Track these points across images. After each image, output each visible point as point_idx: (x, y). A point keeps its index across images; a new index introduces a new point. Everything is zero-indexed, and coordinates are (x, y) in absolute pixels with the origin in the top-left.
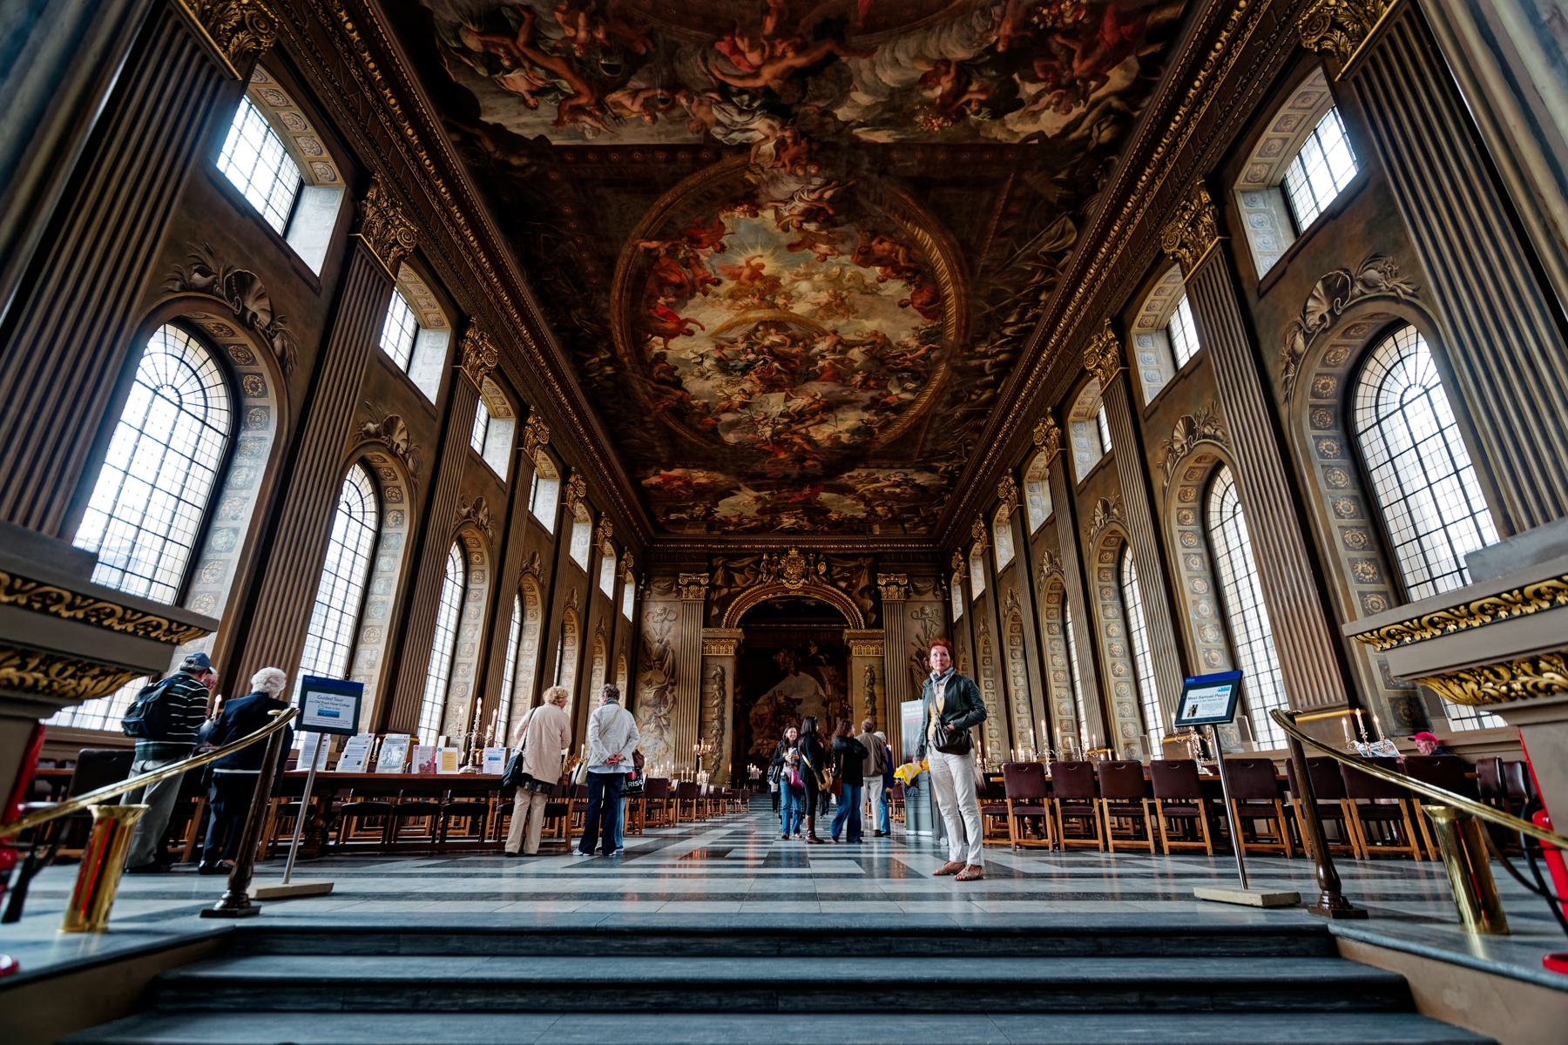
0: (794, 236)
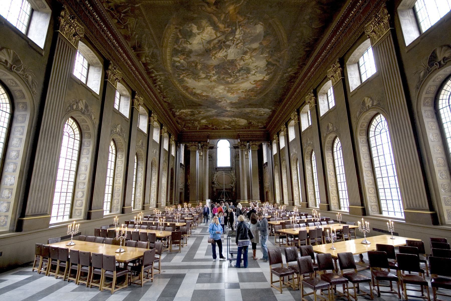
0: (223, 99)
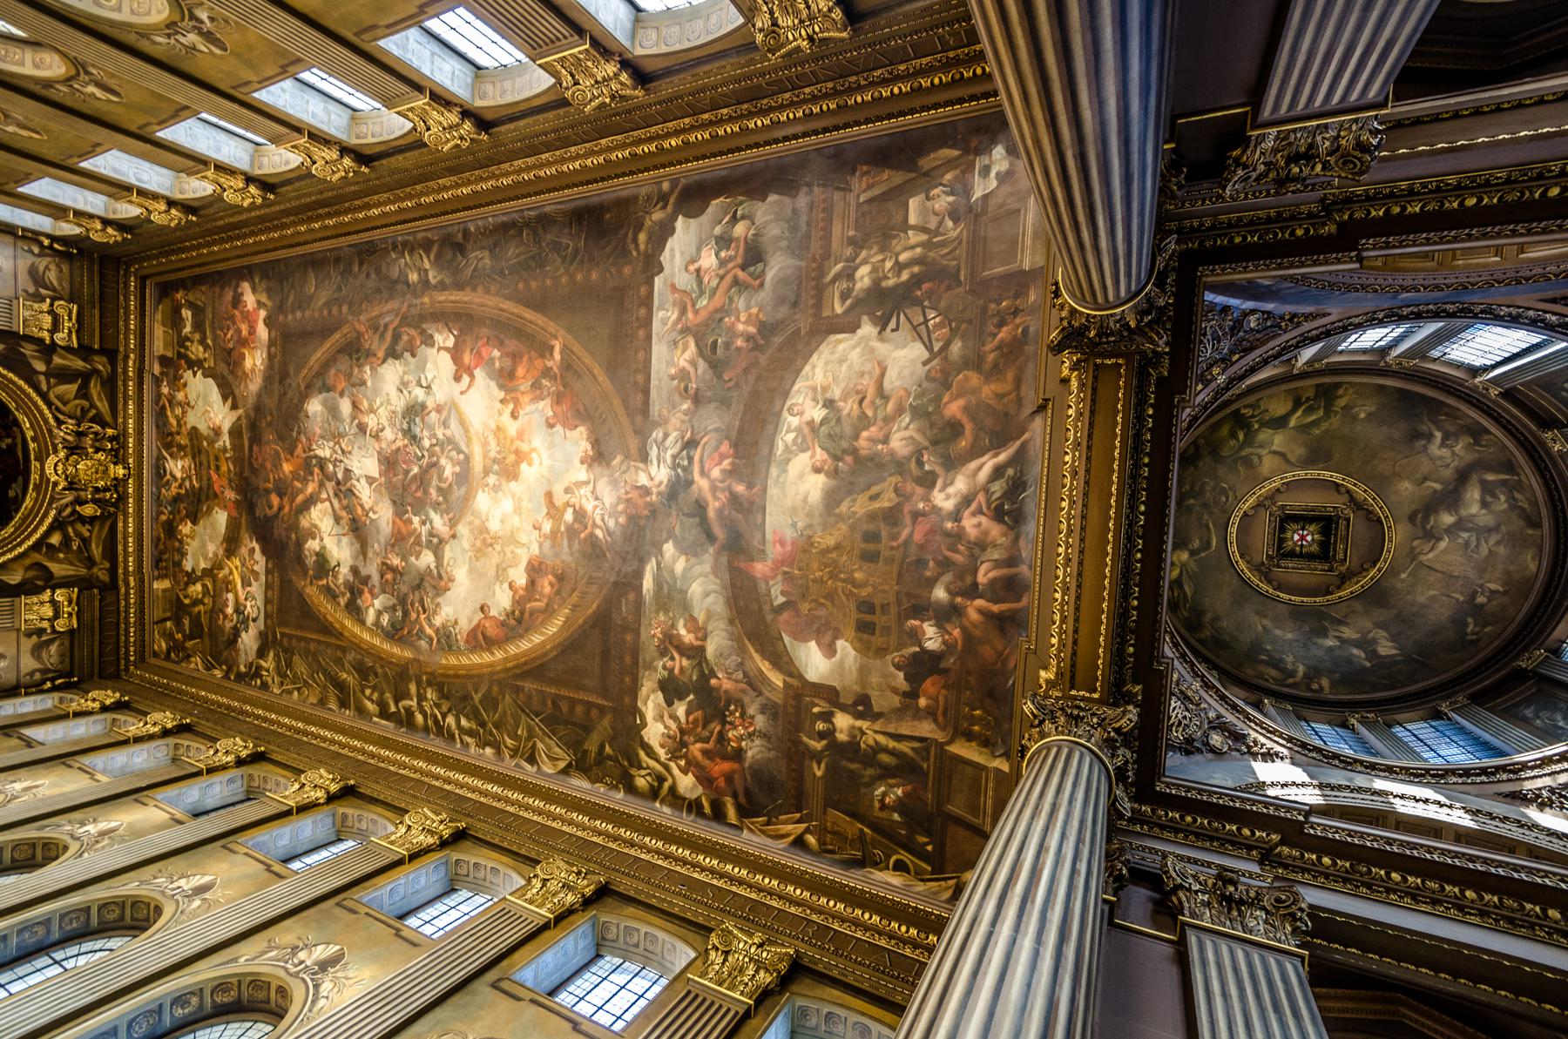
0: (560, 499)
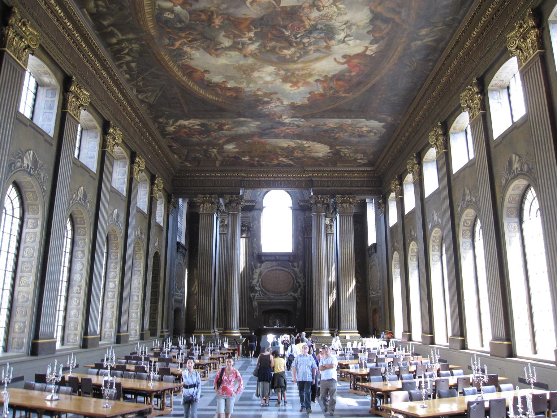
0: (275, 97)
